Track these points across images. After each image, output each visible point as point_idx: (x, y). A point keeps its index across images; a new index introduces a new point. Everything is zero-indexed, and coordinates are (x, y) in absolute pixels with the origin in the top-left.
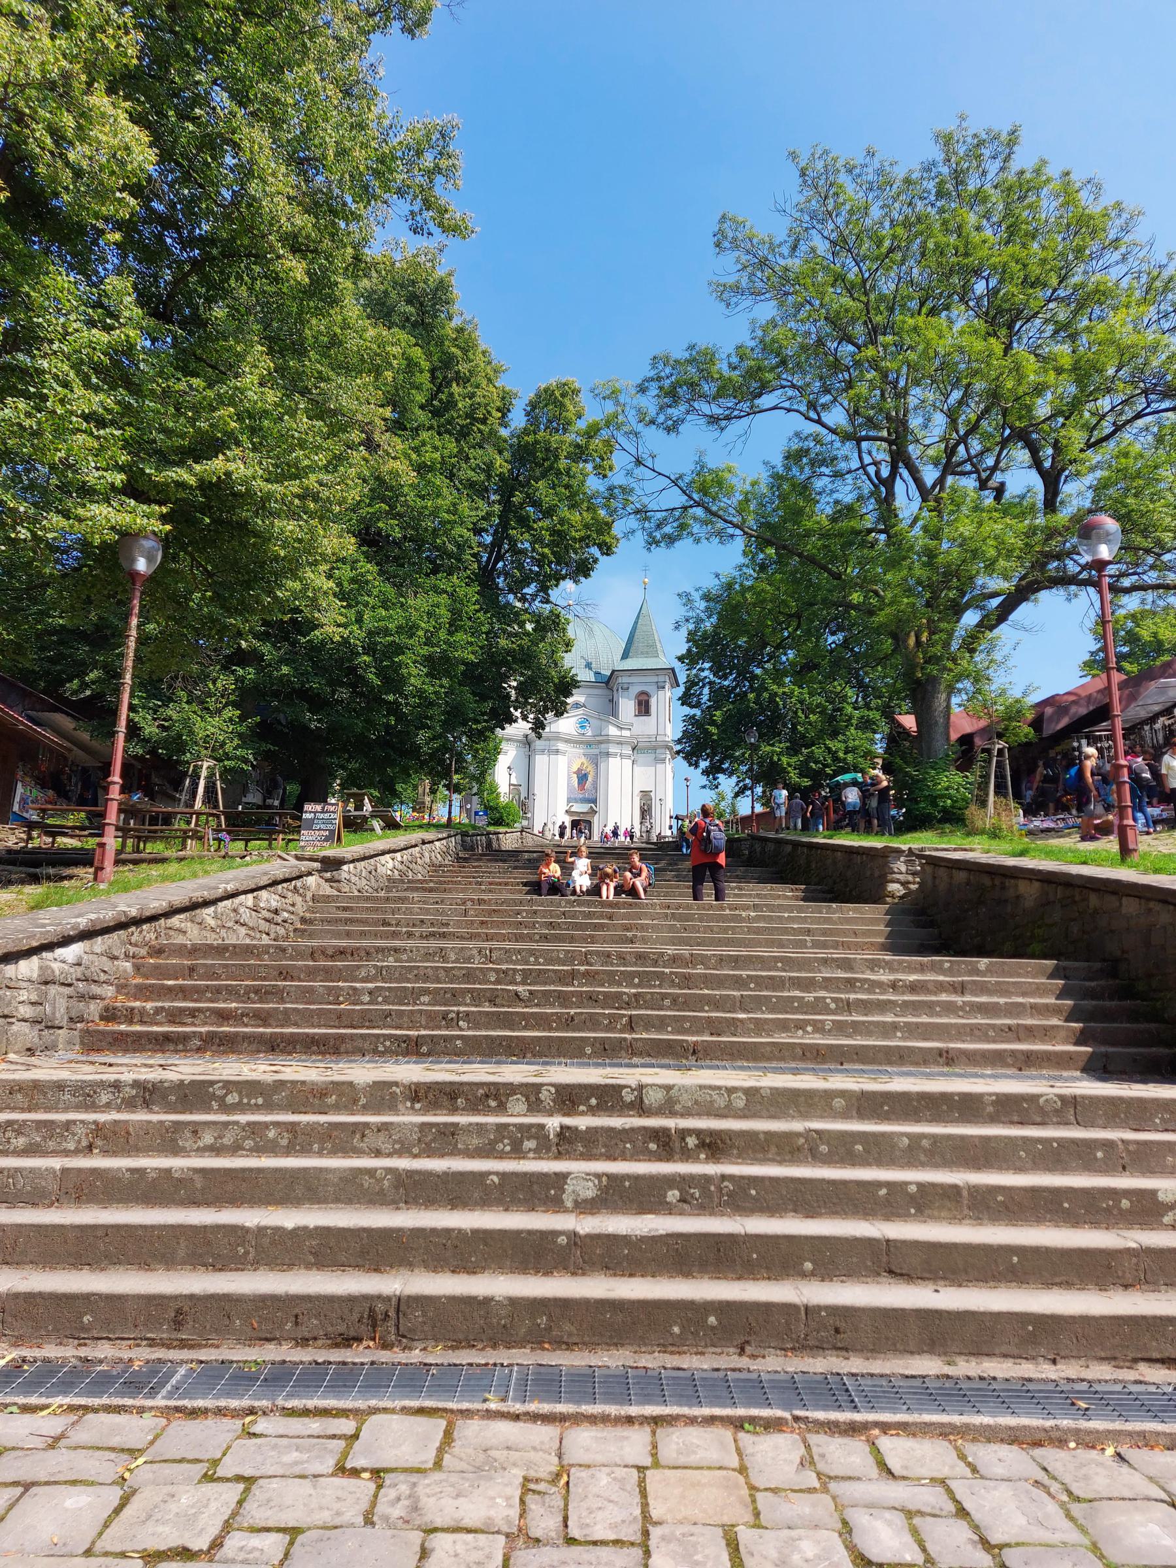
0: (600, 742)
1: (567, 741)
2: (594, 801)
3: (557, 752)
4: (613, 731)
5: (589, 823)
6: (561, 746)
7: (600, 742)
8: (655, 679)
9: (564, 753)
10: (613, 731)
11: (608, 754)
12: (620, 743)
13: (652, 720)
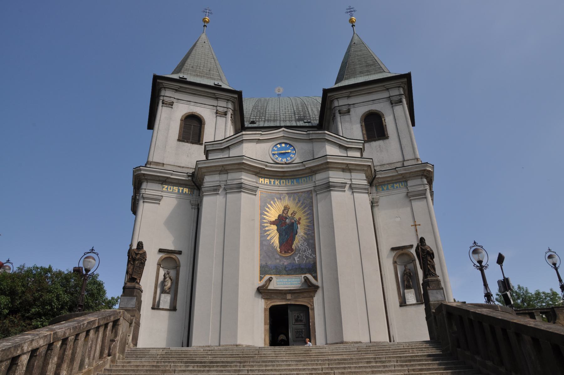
0: (313, 171)
1: (259, 172)
2: (312, 269)
3: (240, 188)
4: (331, 150)
5: (306, 310)
6: (247, 179)
7: (313, 171)
8: (386, 94)
9: (253, 190)
10: (331, 150)
11: (328, 187)
12: (347, 168)
13: (392, 142)
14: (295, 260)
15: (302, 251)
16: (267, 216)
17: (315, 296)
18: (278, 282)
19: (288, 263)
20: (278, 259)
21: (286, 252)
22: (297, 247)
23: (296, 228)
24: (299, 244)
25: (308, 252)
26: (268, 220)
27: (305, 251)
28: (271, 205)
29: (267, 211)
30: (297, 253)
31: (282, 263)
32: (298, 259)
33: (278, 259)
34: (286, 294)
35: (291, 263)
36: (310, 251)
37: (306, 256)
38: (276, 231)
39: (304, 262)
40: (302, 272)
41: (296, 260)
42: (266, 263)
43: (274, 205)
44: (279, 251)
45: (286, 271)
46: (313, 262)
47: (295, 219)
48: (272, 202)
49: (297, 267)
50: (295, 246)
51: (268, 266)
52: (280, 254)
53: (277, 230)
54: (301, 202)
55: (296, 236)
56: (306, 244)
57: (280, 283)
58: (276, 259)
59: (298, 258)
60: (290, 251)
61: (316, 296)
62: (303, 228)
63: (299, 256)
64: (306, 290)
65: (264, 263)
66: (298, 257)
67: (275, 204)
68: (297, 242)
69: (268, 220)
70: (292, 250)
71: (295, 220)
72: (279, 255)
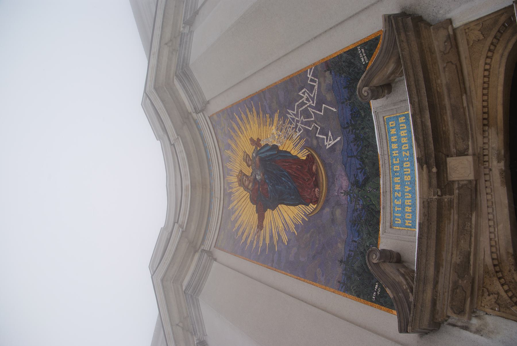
14: (333, 148)
15: (308, 124)
16: (250, 234)
17: (450, 21)
18: (403, 219)
19: (343, 174)
20: (333, 213)
21: (316, 179)
22: (303, 142)
23: (268, 151)
24: (295, 137)
25: (307, 100)
26: (256, 235)
27: (306, 114)
28: (236, 220)
29: (243, 233)
30: (315, 142)
31: (344, 199)
32: (330, 134)
33: (333, 213)
34: (453, 182)
35: (345, 164)
36: (304, 94)
37: (318, 107)
38: (275, 212)
39: (334, 110)
40: (363, 114)
41: (332, 143)
42: (341, 262)
43: (237, 213)
44: (315, 206)
45: (366, 180)
46: (327, 73)
47: (254, 154)
48: (233, 218)
49: (352, 136)
50: (302, 149)
51: (349, 256)
52: (321, 204)
53: (273, 208)
54: (229, 141)
55: (281, 148)
56: (290, 111)
57: (408, 209)
58: (333, 221)
59: (327, 135)
60: (314, 167)
61: (448, 16)
62: (265, 127)
63: (322, 133)
64: (417, 81)
65: (339, 271)
66: (325, 137)
67: (236, 211)
68: (292, 146)
69: (256, 235)
70: (310, 159)
71: (257, 155)
72: (323, 208)
